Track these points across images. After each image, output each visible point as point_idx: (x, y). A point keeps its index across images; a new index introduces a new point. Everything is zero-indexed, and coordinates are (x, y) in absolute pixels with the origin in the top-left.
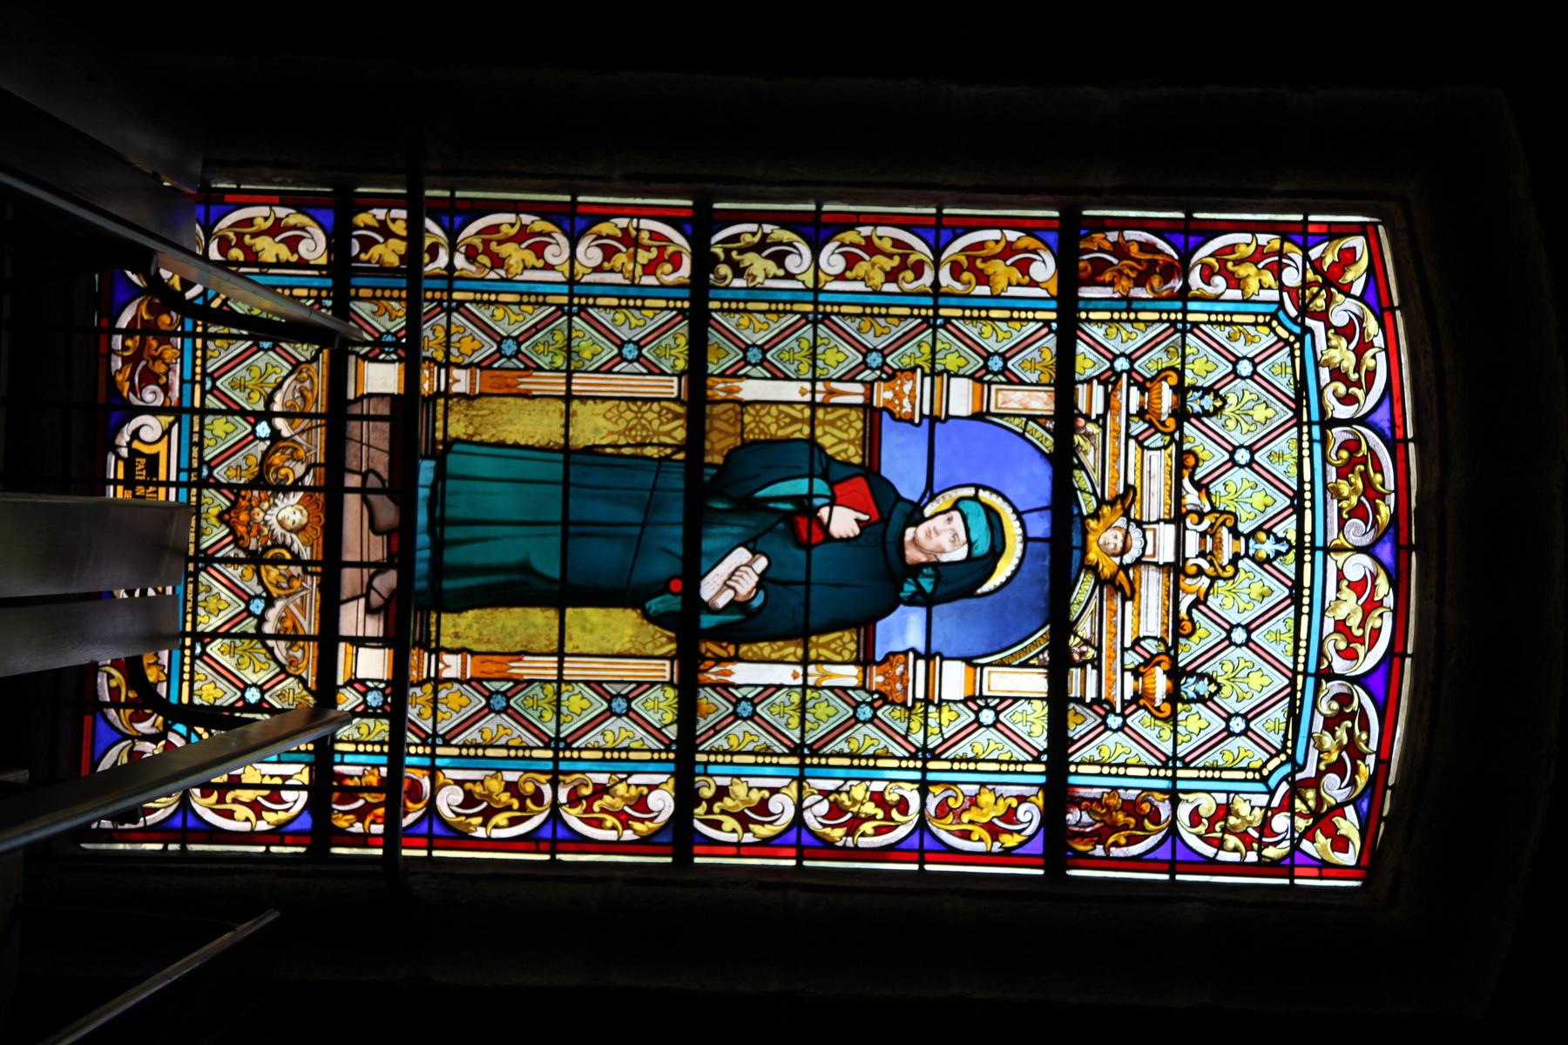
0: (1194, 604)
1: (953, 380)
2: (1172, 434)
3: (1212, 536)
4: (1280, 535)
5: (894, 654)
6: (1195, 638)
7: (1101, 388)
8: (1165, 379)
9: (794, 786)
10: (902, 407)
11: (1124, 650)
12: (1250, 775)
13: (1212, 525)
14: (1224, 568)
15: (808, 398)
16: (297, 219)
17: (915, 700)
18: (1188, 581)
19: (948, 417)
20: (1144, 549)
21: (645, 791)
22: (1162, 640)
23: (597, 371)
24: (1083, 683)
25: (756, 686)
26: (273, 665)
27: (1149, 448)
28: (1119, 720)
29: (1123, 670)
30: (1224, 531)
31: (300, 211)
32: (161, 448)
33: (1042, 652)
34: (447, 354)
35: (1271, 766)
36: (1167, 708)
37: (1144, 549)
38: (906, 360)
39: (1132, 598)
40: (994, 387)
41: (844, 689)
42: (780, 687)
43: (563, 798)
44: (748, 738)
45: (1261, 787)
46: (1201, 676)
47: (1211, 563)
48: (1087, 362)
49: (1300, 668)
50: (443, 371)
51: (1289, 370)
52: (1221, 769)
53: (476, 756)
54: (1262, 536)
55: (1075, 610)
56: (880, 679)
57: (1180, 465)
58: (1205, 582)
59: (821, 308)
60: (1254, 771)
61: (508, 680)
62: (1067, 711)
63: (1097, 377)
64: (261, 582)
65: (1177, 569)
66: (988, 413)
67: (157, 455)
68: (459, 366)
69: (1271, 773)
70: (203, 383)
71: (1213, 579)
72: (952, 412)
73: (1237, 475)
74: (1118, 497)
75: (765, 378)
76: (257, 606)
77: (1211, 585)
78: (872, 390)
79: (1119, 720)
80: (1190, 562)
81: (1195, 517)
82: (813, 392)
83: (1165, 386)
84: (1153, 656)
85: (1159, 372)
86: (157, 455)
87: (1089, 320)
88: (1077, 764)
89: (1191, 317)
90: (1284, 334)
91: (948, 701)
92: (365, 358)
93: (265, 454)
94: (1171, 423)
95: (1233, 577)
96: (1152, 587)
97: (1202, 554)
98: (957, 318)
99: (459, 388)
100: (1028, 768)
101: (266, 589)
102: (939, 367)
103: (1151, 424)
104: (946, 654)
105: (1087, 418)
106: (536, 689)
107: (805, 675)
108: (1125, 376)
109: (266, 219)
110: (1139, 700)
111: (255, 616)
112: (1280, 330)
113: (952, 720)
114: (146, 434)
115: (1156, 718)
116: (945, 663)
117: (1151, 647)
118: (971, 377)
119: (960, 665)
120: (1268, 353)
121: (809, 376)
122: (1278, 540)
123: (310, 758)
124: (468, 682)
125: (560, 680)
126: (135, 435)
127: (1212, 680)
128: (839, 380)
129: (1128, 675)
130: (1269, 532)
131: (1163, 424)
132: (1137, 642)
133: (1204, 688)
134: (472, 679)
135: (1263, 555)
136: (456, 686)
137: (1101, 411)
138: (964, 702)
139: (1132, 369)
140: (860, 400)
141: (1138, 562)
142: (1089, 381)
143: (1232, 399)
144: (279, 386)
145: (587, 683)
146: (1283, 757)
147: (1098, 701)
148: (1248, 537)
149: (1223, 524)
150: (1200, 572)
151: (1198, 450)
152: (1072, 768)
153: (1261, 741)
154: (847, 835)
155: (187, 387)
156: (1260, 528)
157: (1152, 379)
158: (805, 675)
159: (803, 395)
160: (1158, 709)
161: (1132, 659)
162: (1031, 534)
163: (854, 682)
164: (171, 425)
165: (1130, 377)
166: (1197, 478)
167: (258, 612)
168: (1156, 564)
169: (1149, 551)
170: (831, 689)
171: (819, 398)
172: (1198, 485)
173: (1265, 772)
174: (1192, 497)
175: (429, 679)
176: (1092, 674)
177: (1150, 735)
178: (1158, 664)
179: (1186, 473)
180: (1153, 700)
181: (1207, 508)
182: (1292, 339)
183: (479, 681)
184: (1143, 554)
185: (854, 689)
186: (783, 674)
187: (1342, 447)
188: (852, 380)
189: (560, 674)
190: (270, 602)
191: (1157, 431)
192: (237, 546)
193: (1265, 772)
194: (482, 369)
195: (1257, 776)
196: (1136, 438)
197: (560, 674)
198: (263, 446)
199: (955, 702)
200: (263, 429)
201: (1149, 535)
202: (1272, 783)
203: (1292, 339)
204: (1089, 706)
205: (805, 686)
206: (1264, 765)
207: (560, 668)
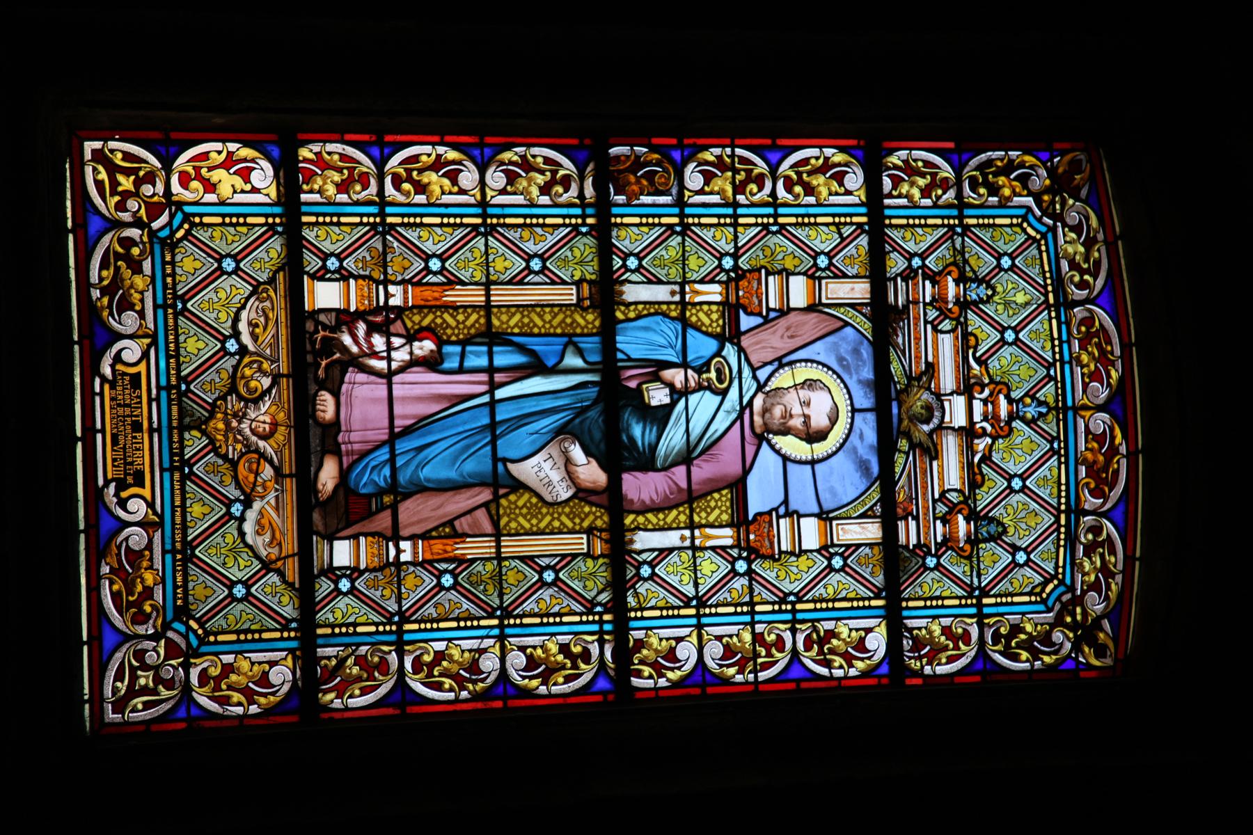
0: (982, 460)
1: (791, 278)
2: (957, 319)
3: (992, 403)
4: (1042, 399)
6: (985, 488)
8: (949, 273)
9: (695, 635)
11: (934, 501)
13: (991, 395)
14: (1001, 428)
16: (246, 152)
17: (781, 552)
18: (976, 441)
21: (673, 643)
22: (960, 491)
23: (510, 282)
26: (256, 562)
28: (935, 560)
29: (935, 519)
30: (1002, 397)
31: (246, 144)
32: (142, 368)
33: (875, 504)
34: (385, 273)
38: (753, 262)
39: (936, 458)
40: (824, 282)
41: (723, 548)
43: (408, 665)
44: (554, 601)
46: (992, 520)
47: (992, 426)
48: (895, 264)
50: (381, 288)
51: (1038, 262)
53: (347, 634)
54: (1028, 400)
55: (898, 470)
57: (966, 346)
58: (989, 440)
63: (900, 274)
64: (238, 486)
65: (969, 433)
66: (820, 304)
67: (139, 374)
68: (394, 283)
70: (174, 306)
71: (994, 439)
73: (1007, 351)
74: (923, 373)
76: (236, 509)
79: (935, 560)
80: (978, 426)
81: (978, 388)
83: (950, 279)
84: (955, 505)
85: (944, 268)
86: (139, 374)
87: (891, 226)
90: (1033, 233)
91: (806, 551)
92: (314, 277)
93: (235, 368)
94: (956, 309)
96: (951, 446)
97: (985, 419)
99: (395, 301)
100: (683, 612)
101: (243, 492)
103: (942, 312)
104: (802, 512)
107: (693, 538)
109: (219, 153)
110: (948, 542)
111: (236, 518)
112: (1030, 230)
114: (128, 356)
115: (961, 557)
116: (802, 520)
117: (953, 497)
118: (805, 274)
120: (1021, 249)
122: (1040, 403)
123: (294, 644)
124: (421, 564)
126: (118, 358)
129: (938, 522)
130: (1033, 398)
131: (950, 310)
132: (943, 493)
133: (993, 528)
134: (424, 561)
135: (1029, 416)
136: (412, 569)
138: (818, 551)
139: (924, 266)
141: (940, 427)
143: (999, 289)
144: (243, 307)
148: (1018, 402)
149: (1000, 392)
150: (984, 433)
151: (977, 332)
153: (1038, 569)
154: (738, 672)
155: (160, 312)
156: (1026, 395)
157: (940, 273)
158: (693, 538)
160: (962, 549)
161: (942, 509)
162: (857, 406)
164: (149, 346)
165: (924, 274)
166: (978, 355)
167: (238, 514)
168: (953, 429)
169: (947, 419)
170: (713, 548)
172: (977, 360)
175: (388, 564)
176: (912, 524)
177: (957, 571)
178: (960, 512)
179: (971, 352)
181: (987, 381)
182: (1038, 237)
183: (430, 562)
185: (731, 547)
187: (1080, 324)
189: (498, 552)
190: (247, 504)
191: (946, 317)
192: (218, 455)
194: (414, 285)
196: (932, 323)
197: (498, 552)
198: (233, 361)
199: (811, 551)
200: (232, 346)
201: (946, 404)
207: (498, 547)
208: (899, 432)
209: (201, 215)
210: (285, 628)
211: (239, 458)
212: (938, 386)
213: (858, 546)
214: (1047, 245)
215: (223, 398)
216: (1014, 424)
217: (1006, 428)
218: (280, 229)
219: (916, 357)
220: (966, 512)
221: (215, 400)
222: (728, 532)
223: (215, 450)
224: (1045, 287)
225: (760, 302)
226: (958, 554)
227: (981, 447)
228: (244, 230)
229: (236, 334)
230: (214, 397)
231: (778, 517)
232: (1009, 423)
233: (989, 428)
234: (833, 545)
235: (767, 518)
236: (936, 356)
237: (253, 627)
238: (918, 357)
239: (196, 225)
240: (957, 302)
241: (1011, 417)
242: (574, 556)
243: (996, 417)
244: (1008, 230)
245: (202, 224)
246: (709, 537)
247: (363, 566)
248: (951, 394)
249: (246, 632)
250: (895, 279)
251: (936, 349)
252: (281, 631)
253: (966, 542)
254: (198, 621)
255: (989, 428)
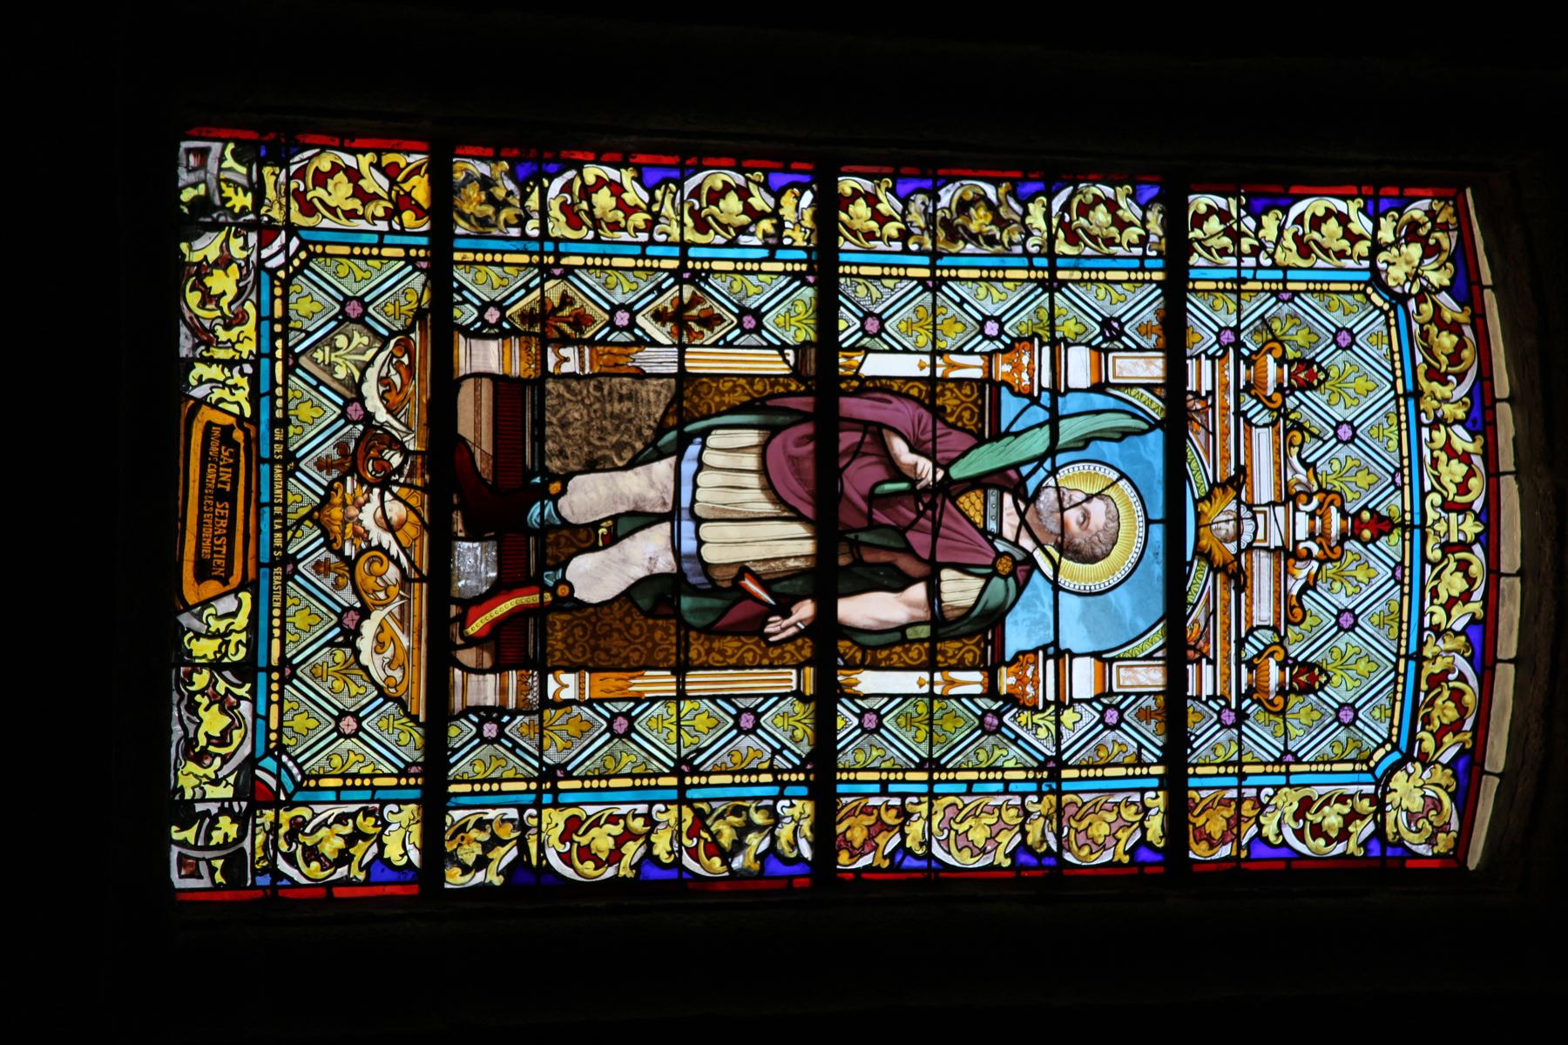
0: (1303, 591)
1: (1071, 350)
2: (1278, 410)
4: (1384, 513)
5: (1024, 653)
7: (1209, 363)
8: (1270, 351)
10: (1021, 380)
12: (1358, 767)
13: (1320, 506)
14: (1331, 549)
15: (926, 373)
19: (1068, 390)
20: (1255, 533)
24: (1203, 680)
25: (882, 695)
26: (371, 688)
27: (1257, 426)
30: (1333, 509)
35: (1377, 757)
36: (1279, 700)
37: (1255, 533)
40: (1111, 356)
41: (971, 697)
42: (906, 697)
45: (1369, 778)
47: (1321, 546)
48: (1202, 336)
49: (1403, 651)
51: (1386, 340)
52: (1331, 763)
56: (1012, 680)
58: (1315, 564)
59: (938, 273)
60: (1362, 762)
61: (628, 700)
62: (1186, 708)
64: (356, 591)
66: (1108, 384)
69: (1377, 764)
71: (1322, 562)
72: (1071, 385)
74: (1236, 477)
75: (884, 351)
77: (1320, 569)
78: (990, 362)
80: (1301, 546)
81: (1304, 498)
82: (933, 366)
84: (1267, 647)
88: (1195, 766)
89: (1290, 286)
95: (1339, 559)
96: (1262, 568)
97: (1312, 536)
98: (1074, 282)
101: (360, 599)
102: (1058, 335)
103: (1259, 401)
105: (1197, 394)
106: (657, 709)
108: (1231, 350)
113: (1077, 721)
115: (1270, 712)
117: (1267, 636)
118: (1088, 344)
119: (1089, 661)
121: (929, 348)
125: (681, 695)
127: (1322, 671)
128: (959, 351)
131: (1269, 399)
132: (1250, 631)
137: (1209, 388)
138: (1089, 702)
140: (978, 374)
141: (1250, 547)
142: (1198, 357)
143: (1333, 373)
145: (713, 699)
146: (1388, 747)
147: (1214, 697)
149: (1332, 503)
150: (1309, 556)
152: (1191, 771)
156: (1365, 507)
159: (922, 368)
163: (978, 689)
168: (1267, 549)
169: (1260, 535)
170: (958, 698)
171: (939, 373)
172: (1303, 462)
173: (1372, 764)
174: (1302, 474)
176: (1207, 670)
178: (1271, 655)
180: (1268, 693)
184: (1254, 539)
185: (980, 696)
186: (908, 682)
188: (971, 352)
190: (365, 613)
191: (1265, 407)
192: (331, 550)
193: (1372, 764)
195: (1365, 768)
201: (1260, 517)
202: (1379, 773)
203: (1386, 307)
204: (1206, 703)
205: (931, 696)
206: (1370, 757)
208: (1195, 553)
209: (324, 244)
210: (402, 773)
211: (359, 555)
212: (1251, 493)
213: (1139, 695)
214: (1396, 317)
215: (342, 479)
216: (1347, 545)
217: (1338, 550)
218: (424, 265)
219: (1223, 458)
220: (1280, 656)
221: (331, 483)
222: (977, 676)
223: (328, 544)
224: (1393, 372)
225: (1031, 379)
226: (1266, 710)
227: (1305, 572)
228: (376, 263)
229: (361, 399)
230: (329, 478)
231: (1046, 658)
232: (1341, 543)
233: (1315, 550)
234: (1111, 693)
235: (1031, 657)
236: (1249, 456)
237: (364, 771)
238: (1226, 458)
239: (317, 255)
240: (1279, 388)
241: (1344, 537)
242: (782, 696)
243: (1325, 534)
244: (1349, 298)
245: (324, 255)
246: (953, 683)
247: (512, 704)
248: (1273, 504)
249: (354, 776)
250: (1198, 357)
251: (1249, 447)
252: (398, 776)
253: (1278, 694)
254: (293, 759)
255: (1315, 550)
